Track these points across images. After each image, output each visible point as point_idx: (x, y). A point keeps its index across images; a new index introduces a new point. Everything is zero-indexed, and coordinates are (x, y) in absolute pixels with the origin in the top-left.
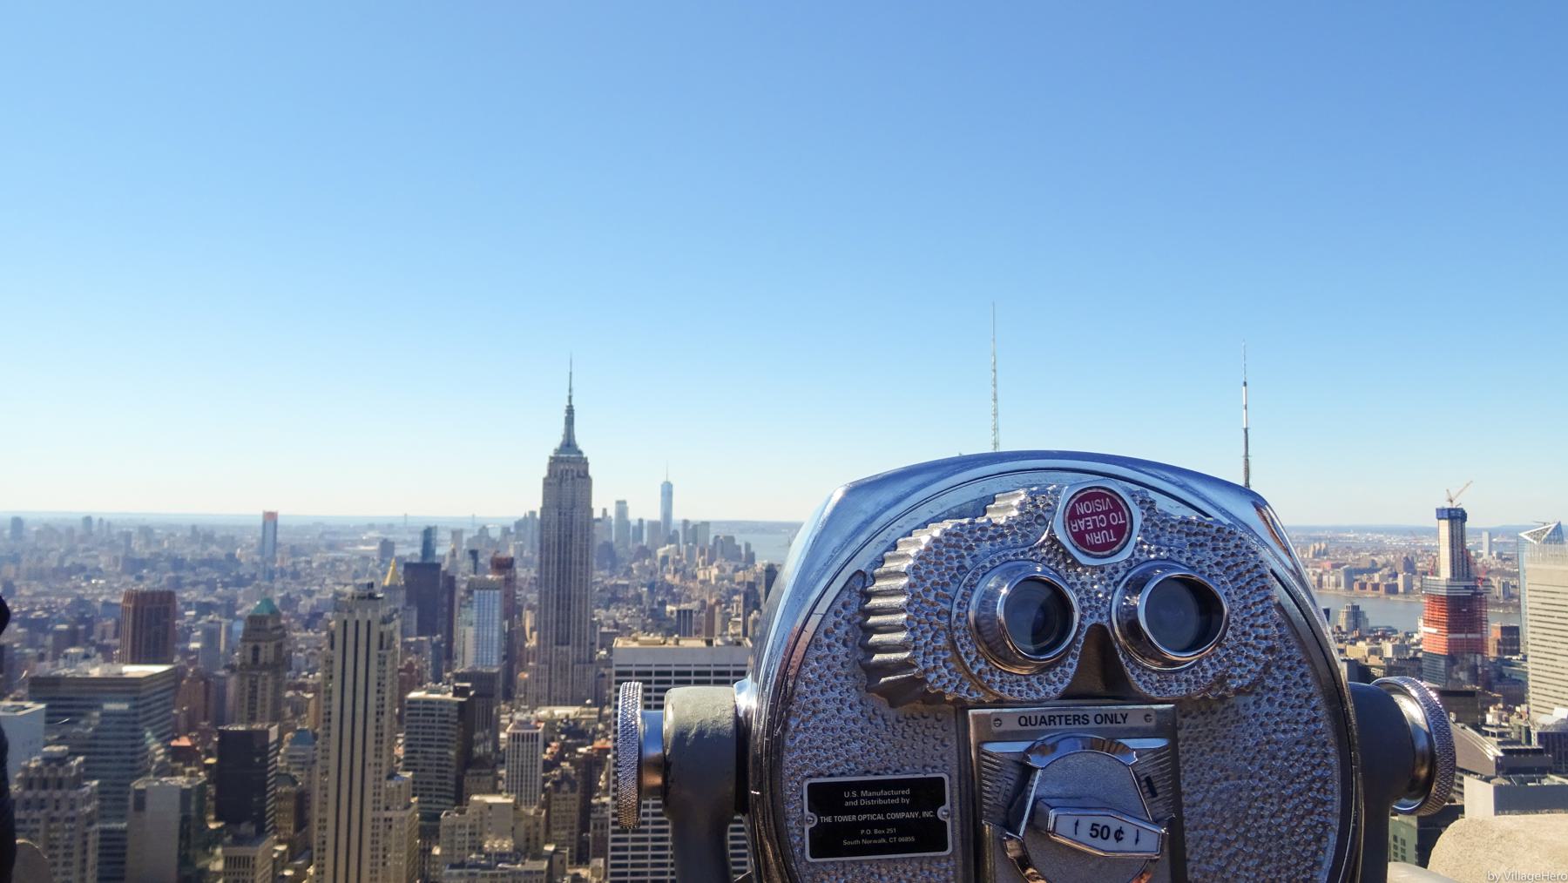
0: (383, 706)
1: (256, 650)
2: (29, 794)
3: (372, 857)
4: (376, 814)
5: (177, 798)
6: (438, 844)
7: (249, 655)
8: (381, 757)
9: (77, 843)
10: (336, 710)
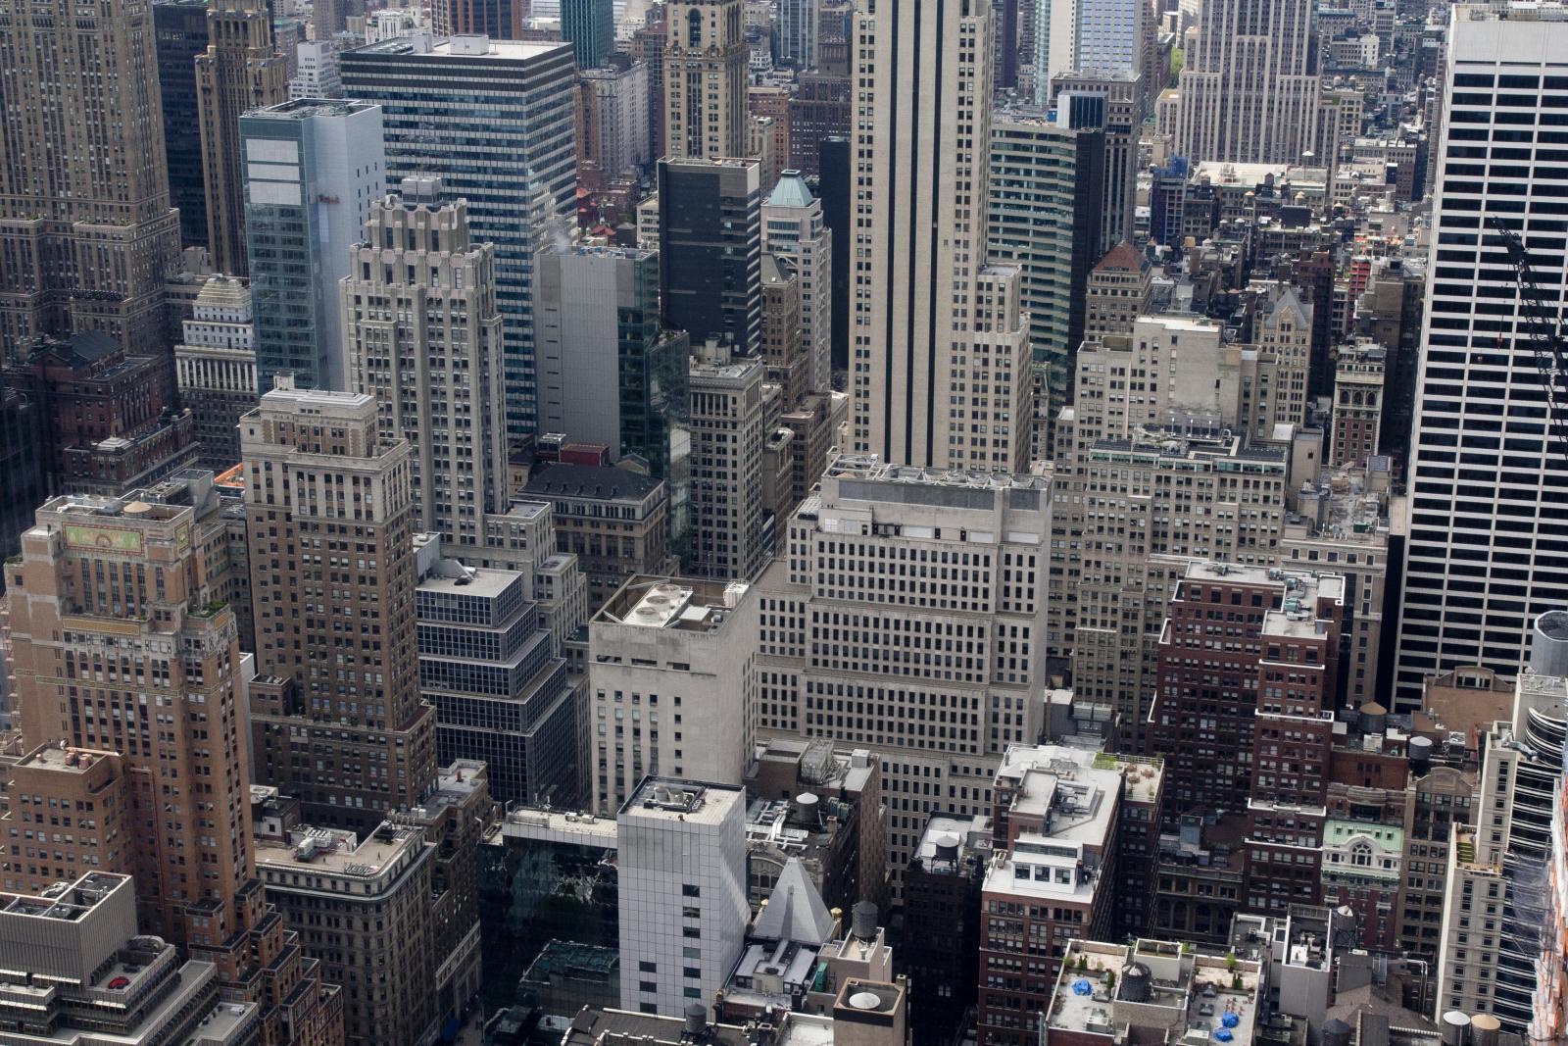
0: (969, 130)
1: (695, 18)
2: (390, 257)
3: (953, 414)
4: (959, 336)
5: (610, 283)
6: (1070, 402)
7: (684, 27)
8: (967, 228)
9: (470, 346)
10: (881, 134)
